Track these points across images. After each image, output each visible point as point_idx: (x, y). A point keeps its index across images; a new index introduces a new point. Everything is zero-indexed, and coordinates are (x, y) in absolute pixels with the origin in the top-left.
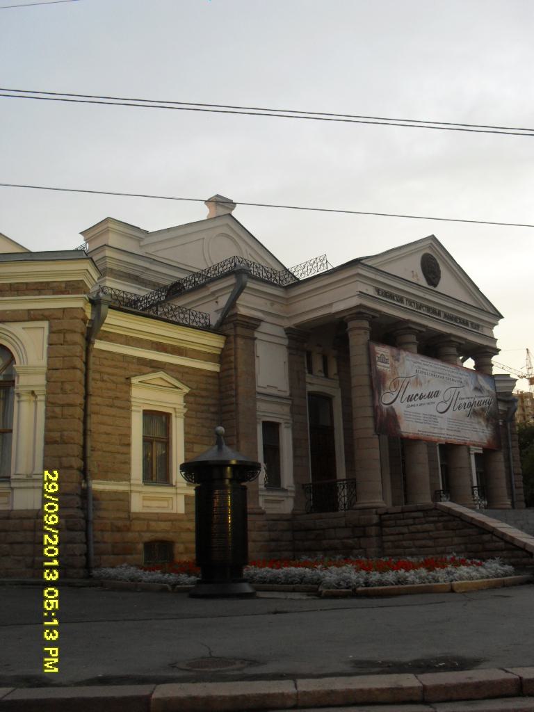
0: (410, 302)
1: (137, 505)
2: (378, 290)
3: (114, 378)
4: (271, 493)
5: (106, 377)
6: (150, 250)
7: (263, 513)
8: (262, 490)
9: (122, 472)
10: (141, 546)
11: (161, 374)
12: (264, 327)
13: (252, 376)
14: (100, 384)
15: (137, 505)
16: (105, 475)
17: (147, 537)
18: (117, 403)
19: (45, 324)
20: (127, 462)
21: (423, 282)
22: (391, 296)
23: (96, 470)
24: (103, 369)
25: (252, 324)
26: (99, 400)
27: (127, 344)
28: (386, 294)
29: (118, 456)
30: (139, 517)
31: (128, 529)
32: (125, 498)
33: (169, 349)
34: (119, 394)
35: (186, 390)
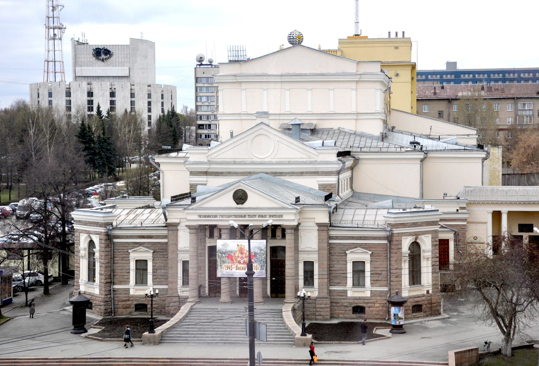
0: (222, 216)
1: (132, 292)
2: (200, 216)
3: (122, 251)
4: (185, 288)
5: (120, 251)
6: (213, 156)
7: (179, 296)
8: (179, 287)
9: (127, 282)
10: (133, 306)
11: (141, 247)
12: (180, 225)
13: (176, 244)
14: (118, 253)
15: (132, 292)
16: (120, 283)
17: (135, 303)
18: (125, 259)
19: (98, 236)
20: (129, 278)
21: (233, 204)
22: (209, 216)
23: (117, 282)
24: (118, 248)
25: (176, 225)
26: (117, 259)
27: (127, 238)
28: (205, 216)
29: (125, 277)
30: (132, 296)
31: (129, 300)
32: (128, 290)
33: (145, 237)
34: (125, 256)
35: (152, 251)
